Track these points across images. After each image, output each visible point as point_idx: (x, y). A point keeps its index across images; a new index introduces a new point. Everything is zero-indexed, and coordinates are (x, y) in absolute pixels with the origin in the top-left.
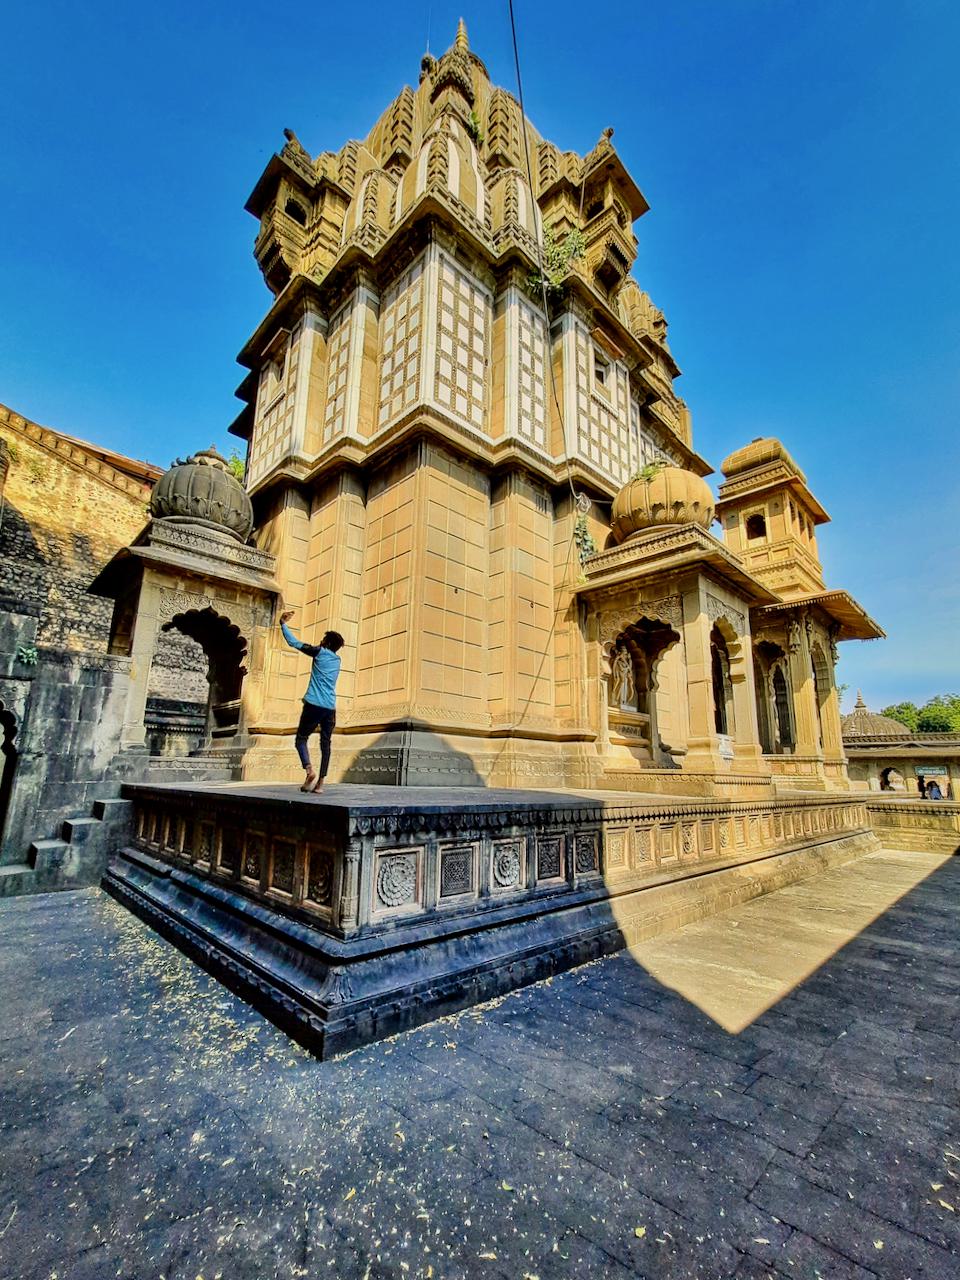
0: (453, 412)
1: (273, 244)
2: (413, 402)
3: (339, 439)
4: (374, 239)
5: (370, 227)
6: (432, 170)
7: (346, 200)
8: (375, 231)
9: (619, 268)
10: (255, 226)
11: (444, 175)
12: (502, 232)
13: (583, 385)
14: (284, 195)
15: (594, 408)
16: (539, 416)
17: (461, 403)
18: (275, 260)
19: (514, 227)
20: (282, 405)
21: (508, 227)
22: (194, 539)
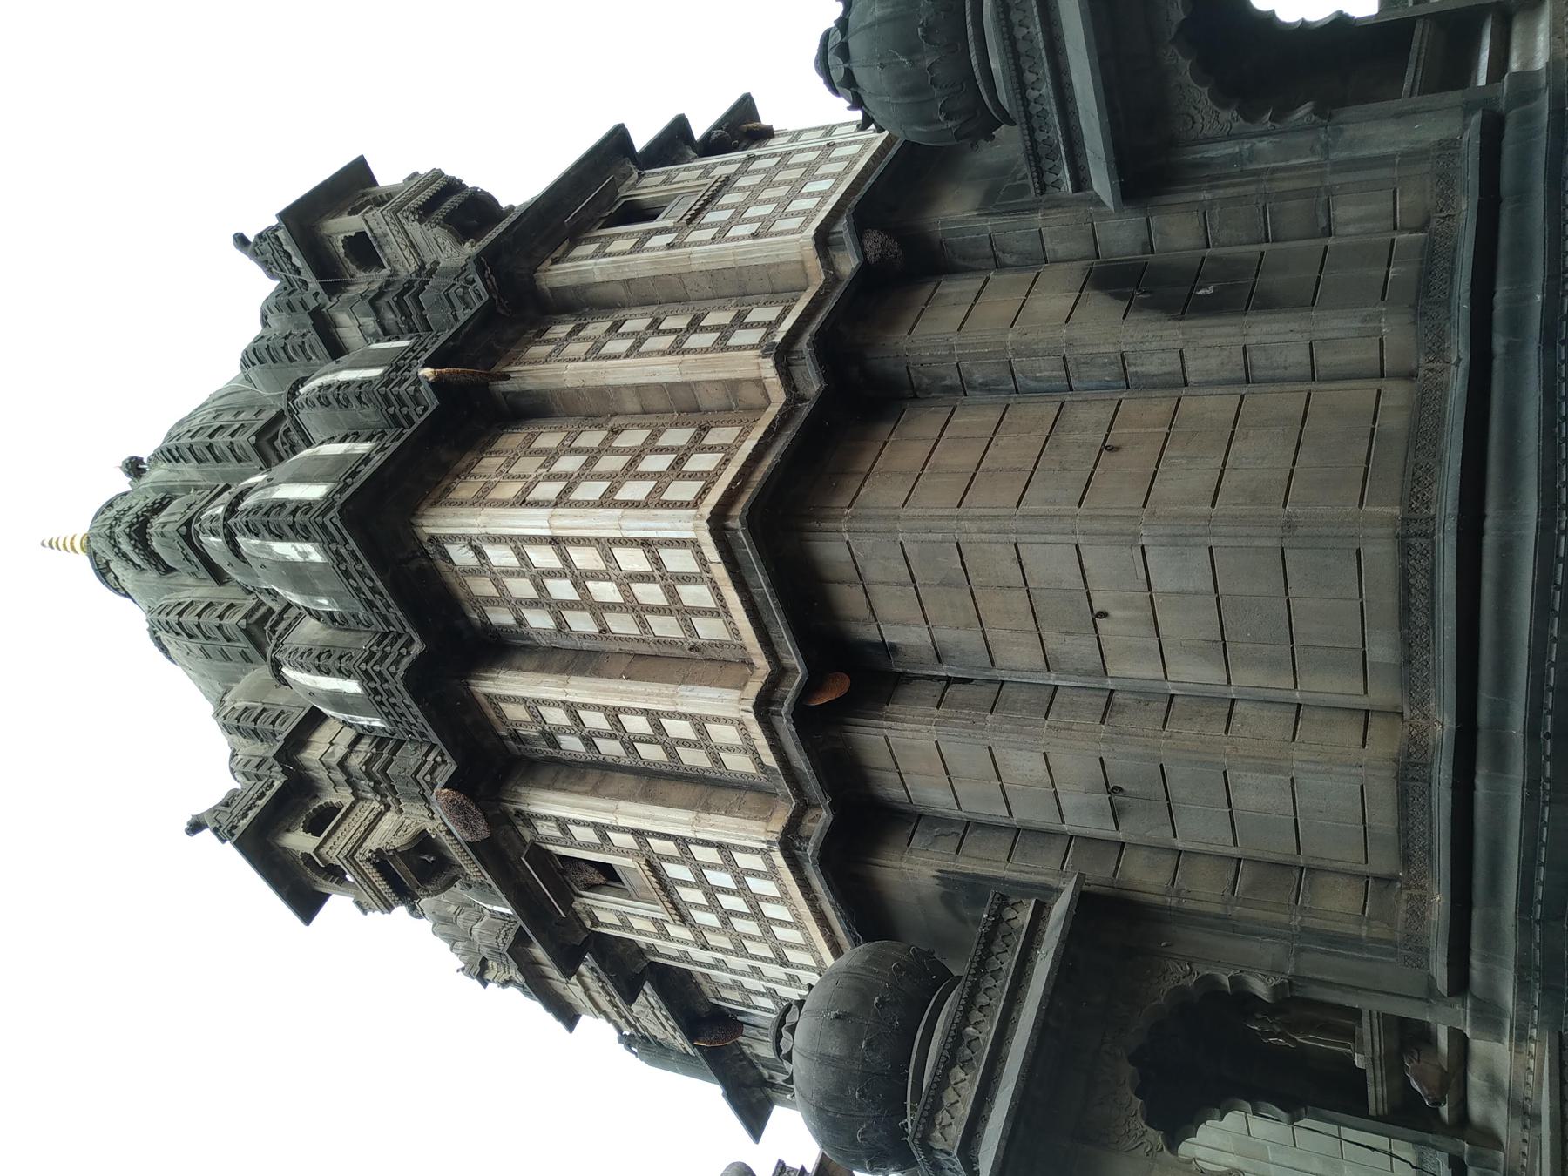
0: (718, 476)
1: (375, 866)
3: (756, 731)
4: (385, 656)
5: (366, 661)
6: (287, 530)
7: (314, 719)
8: (372, 654)
10: (339, 906)
11: (297, 508)
12: (391, 410)
13: (669, 238)
14: (299, 841)
15: (711, 217)
16: (724, 317)
17: (701, 462)
18: (400, 868)
19: (386, 385)
20: (675, 871)
21: (385, 397)
22: (970, 1029)
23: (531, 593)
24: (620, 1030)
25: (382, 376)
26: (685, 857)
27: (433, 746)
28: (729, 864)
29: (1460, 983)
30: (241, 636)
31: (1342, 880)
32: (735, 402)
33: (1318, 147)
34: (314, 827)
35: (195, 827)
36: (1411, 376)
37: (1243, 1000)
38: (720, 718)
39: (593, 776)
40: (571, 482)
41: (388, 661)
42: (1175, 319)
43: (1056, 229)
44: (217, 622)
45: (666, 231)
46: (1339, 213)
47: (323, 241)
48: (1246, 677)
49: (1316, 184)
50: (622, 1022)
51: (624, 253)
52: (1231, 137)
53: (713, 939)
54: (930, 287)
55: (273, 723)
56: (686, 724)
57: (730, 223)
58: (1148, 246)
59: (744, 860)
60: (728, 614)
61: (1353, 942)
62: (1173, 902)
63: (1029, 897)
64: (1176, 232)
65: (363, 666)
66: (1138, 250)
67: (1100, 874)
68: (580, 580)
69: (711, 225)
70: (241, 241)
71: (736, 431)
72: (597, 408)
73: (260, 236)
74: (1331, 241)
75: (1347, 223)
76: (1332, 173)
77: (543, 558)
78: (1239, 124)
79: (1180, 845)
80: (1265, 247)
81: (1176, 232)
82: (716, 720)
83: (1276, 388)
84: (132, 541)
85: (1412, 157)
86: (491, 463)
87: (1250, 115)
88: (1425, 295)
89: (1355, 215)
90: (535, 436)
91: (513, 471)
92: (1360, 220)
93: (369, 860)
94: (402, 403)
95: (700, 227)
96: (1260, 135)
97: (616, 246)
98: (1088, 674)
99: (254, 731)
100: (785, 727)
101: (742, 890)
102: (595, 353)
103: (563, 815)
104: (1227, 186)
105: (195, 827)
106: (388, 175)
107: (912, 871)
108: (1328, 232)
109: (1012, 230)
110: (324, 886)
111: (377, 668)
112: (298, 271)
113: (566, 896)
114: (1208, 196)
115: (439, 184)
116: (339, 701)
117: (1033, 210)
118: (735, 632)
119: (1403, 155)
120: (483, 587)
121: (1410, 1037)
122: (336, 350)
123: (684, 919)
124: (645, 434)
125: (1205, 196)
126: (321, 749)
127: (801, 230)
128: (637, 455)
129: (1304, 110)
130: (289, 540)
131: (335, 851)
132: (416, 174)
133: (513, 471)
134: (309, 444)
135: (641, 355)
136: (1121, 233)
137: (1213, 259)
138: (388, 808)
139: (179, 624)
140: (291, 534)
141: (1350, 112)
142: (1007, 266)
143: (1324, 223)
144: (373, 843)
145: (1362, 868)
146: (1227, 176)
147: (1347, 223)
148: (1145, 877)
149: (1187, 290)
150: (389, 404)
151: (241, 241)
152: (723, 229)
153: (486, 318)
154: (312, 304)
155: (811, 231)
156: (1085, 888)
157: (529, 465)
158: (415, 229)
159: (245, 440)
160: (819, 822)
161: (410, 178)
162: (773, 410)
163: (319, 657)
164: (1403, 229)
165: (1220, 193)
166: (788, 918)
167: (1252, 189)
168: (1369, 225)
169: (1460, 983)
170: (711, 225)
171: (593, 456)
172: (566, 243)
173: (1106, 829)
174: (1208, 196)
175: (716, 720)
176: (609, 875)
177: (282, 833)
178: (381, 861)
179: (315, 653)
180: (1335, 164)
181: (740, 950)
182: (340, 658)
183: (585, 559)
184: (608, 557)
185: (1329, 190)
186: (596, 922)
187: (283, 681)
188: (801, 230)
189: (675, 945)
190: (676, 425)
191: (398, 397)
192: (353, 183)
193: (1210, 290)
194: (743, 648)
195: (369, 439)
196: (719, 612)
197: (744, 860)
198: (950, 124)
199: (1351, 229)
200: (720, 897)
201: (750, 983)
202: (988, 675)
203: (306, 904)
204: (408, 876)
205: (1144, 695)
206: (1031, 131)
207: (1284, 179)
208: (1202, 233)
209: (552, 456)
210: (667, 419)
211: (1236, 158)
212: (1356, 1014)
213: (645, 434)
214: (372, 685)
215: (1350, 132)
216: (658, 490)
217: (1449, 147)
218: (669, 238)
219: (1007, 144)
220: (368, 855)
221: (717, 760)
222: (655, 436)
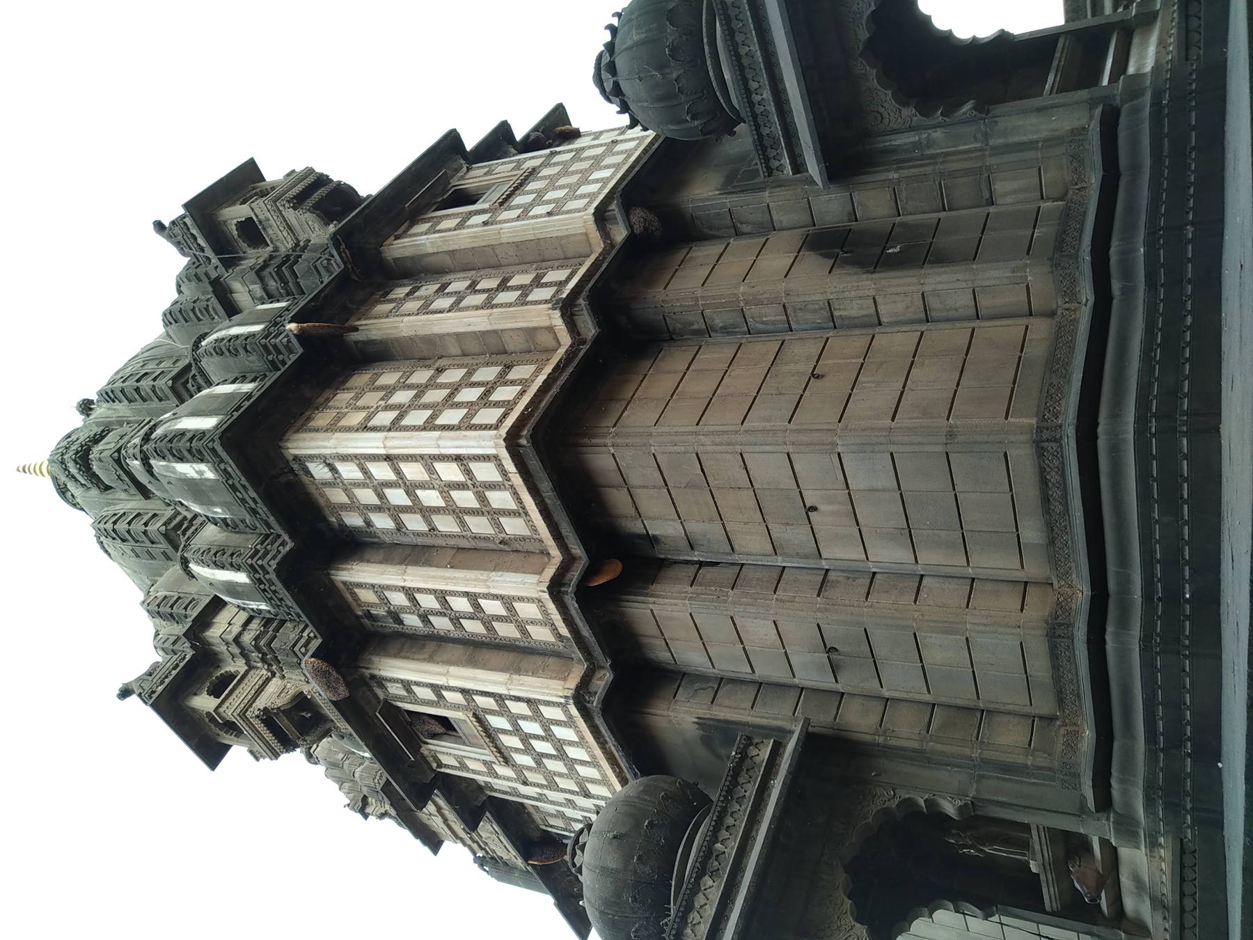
0: (516, 404)
1: (263, 721)
2: (500, 466)
3: (551, 606)
4: (267, 553)
5: (252, 557)
6: (186, 454)
7: (216, 605)
9: (322, 192)
10: (238, 754)
11: (194, 436)
12: (270, 357)
13: (485, 217)
14: (204, 702)
15: (519, 200)
16: (526, 279)
17: (504, 393)
18: (283, 723)
19: (266, 337)
20: (497, 722)
21: (265, 347)
23: (374, 500)
24: (474, 853)
25: (264, 330)
26: (503, 712)
27: (306, 626)
28: (537, 716)
29: (1104, 802)
30: (162, 539)
31: (1016, 720)
32: (534, 344)
33: (979, 136)
34: (215, 692)
35: (125, 693)
36: (1052, 314)
37: (936, 818)
38: (522, 597)
39: (431, 646)
40: (403, 410)
41: (269, 557)
42: (868, 272)
43: (779, 203)
44: (143, 528)
45: (483, 212)
46: (999, 187)
47: (219, 224)
48: (929, 558)
49: (978, 165)
50: (475, 846)
51: (450, 230)
52: (911, 129)
53: (532, 777)
54: (685, 251)
55: (186, 608)
56: (498, 603)
57: (532, 205)
58: (853, 216)
59: (549, 713)
60: (526, 514)
61: (1021, 770)
62: (881, 740)
63: (768, 738)
64: (873, 204)
65: (249, 561)
66: (846, 219)
67: (822, 719)
68: (411, 489)
69: (518, 207)
70: (159, 226)
71: (533, 368)
72: (427, 352)
73: (173, 223)
74: (992, 209)
75: (1004, 195)
76: (990, 156)
77: (382, 472)
78: (918, 119)
79: (886, 694)
80: (942, 215)
81: (873, 204)
82: (521, 599)
83: (947, 325)
84: (79, 466)
85: (1051, 142)
86: (343, 397)
87: (925, 111)
88: (1061, 250)
89: (1011, 190)
90: (378, 376)
91: (360, 403)
92: (1015, 192)
93: (257, 717)
94: (279, 352)
95: (509, 208)
96: (935, 127)
97: (445, 224)
98: (807, 557)
99: (171, 615)
100: (573, 605)
101: (548, 737)
102: (425, 309)
103: (408, 678)
104: (910, 167)
105: (125, 693)
106: (273, 172)
107: (677, 718)
108: (991, 202)
109: (746, 205)
110: (226, 739)
111: (260, 562)
112: (202, 250)
113: (415, 744)
114: (896, 176)
115: (310, 179)
116: (232, 589)
117: (763, 189)
118: (534, 529)
119: (1045, 140)
120: (338, 496)
121: (1071, 847)
122: (231, 310)
123: (507, 761)
124: (463, 371)
125: (894, 175)
126: (221, 629)
127: (584, 209)
128: (456, 388)
129: (967, 107)
130: (188, 461)
131: (231, 710)
132: (293, 171)
133: (360, 403)
134: (209, 384)
135: (460, 310)
136: (831, 206)
137: (902, 225)
138: (274, 675)
139: (114, 530)
140: (189, 457)
141: (1001, 109)
142: (744, 234)
143: (987, 195)
144: (261, 703)
145: (1028, 710)
146: (911, 160)
147: (1004, 195)
148: (859, 720)
149: (878, 250)
150: (269, 353)
151: (159, 226)
152: (527, 208)
153: (342, 283)
154: (214, 275)
155: (592, 210)
156: (810, 729)
157: (371, 399)
158: (290, 214)
159: (164, 383)
160: (603, 680)
161: (288, 175)
162: (561, 351)
163: (215, 554)
164: (1048, 199)
165: (906, 172)
166: (587, 758)
167: (928, 169)
168: (1021, 196)
169: (1104, 802)
170: (518, 207)
171: (421, 390)
172: (406, 224)
173: (827, 682)
174: (896, 176)
175: (521, 599)
176: (446, 727)
177: (190, 698)
178: (268, 718)
179: (213, 552)
180: (993, 148)
181: (552, 785)
182: (232, 555)
183: (413, 472)
184: (431, 471)
185: (988, 169)
186: (440, 765)
187: (191, 575)
188: (584, 209)
189: (503, 781)
190: (487, 364)
191: (275, 346)
192: (245, 180)
193: (897, 249)
194: (541, 541)
195: (253, 380)
196: (519, 513)
197: (549, 713)
198: (696, 123)
199: (1009, 200)
200: (533, 742)
201: (569, 812)
202: (730, 559)
203: (212, 753)
204: (290, 728)
205: (852, 573)
206: (757, 127)
207: (953, 161)
208: (893, 203)
209: (390, 390)
210: (480, 360)
211: (917, 145)
212: (1026, 828)
213: (463, 371)
214: (257, 576)
215: (1003, 123)
216: (469, 416)
217: (1079, 134)
218: (485, 217)
219: (742, 140)
220: (257, 713)
221: (524, 632)
222: (470, 373)
